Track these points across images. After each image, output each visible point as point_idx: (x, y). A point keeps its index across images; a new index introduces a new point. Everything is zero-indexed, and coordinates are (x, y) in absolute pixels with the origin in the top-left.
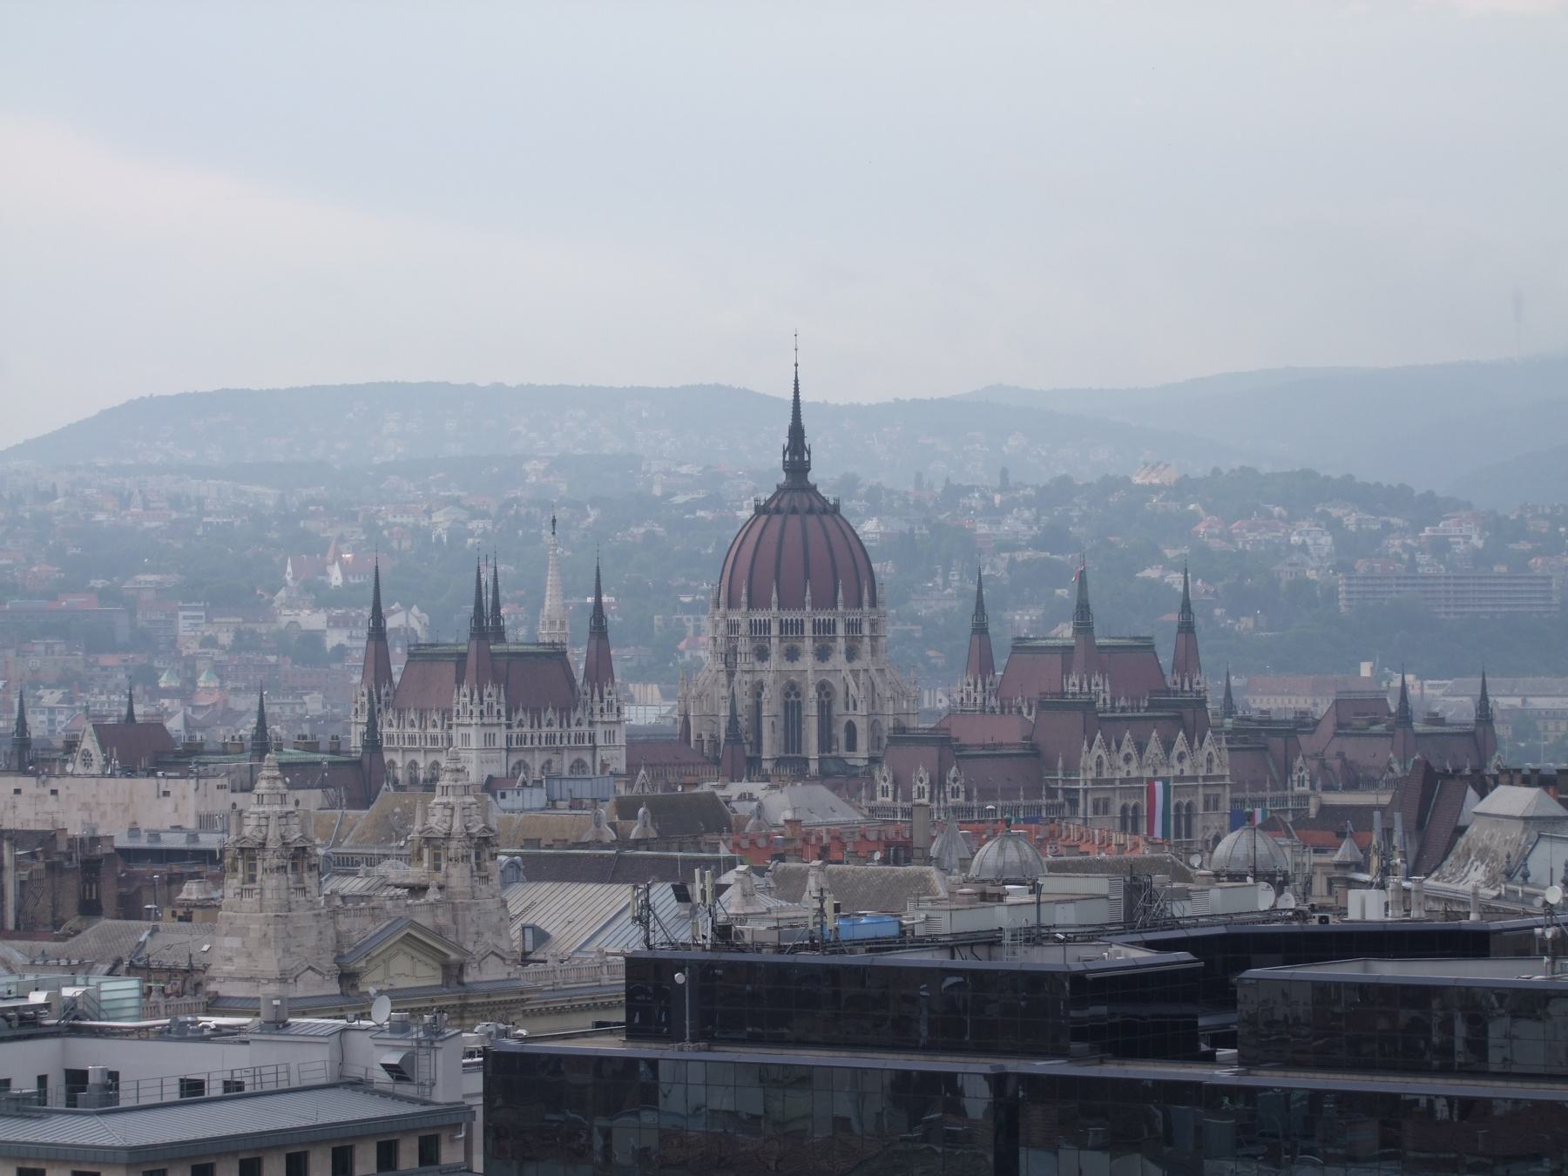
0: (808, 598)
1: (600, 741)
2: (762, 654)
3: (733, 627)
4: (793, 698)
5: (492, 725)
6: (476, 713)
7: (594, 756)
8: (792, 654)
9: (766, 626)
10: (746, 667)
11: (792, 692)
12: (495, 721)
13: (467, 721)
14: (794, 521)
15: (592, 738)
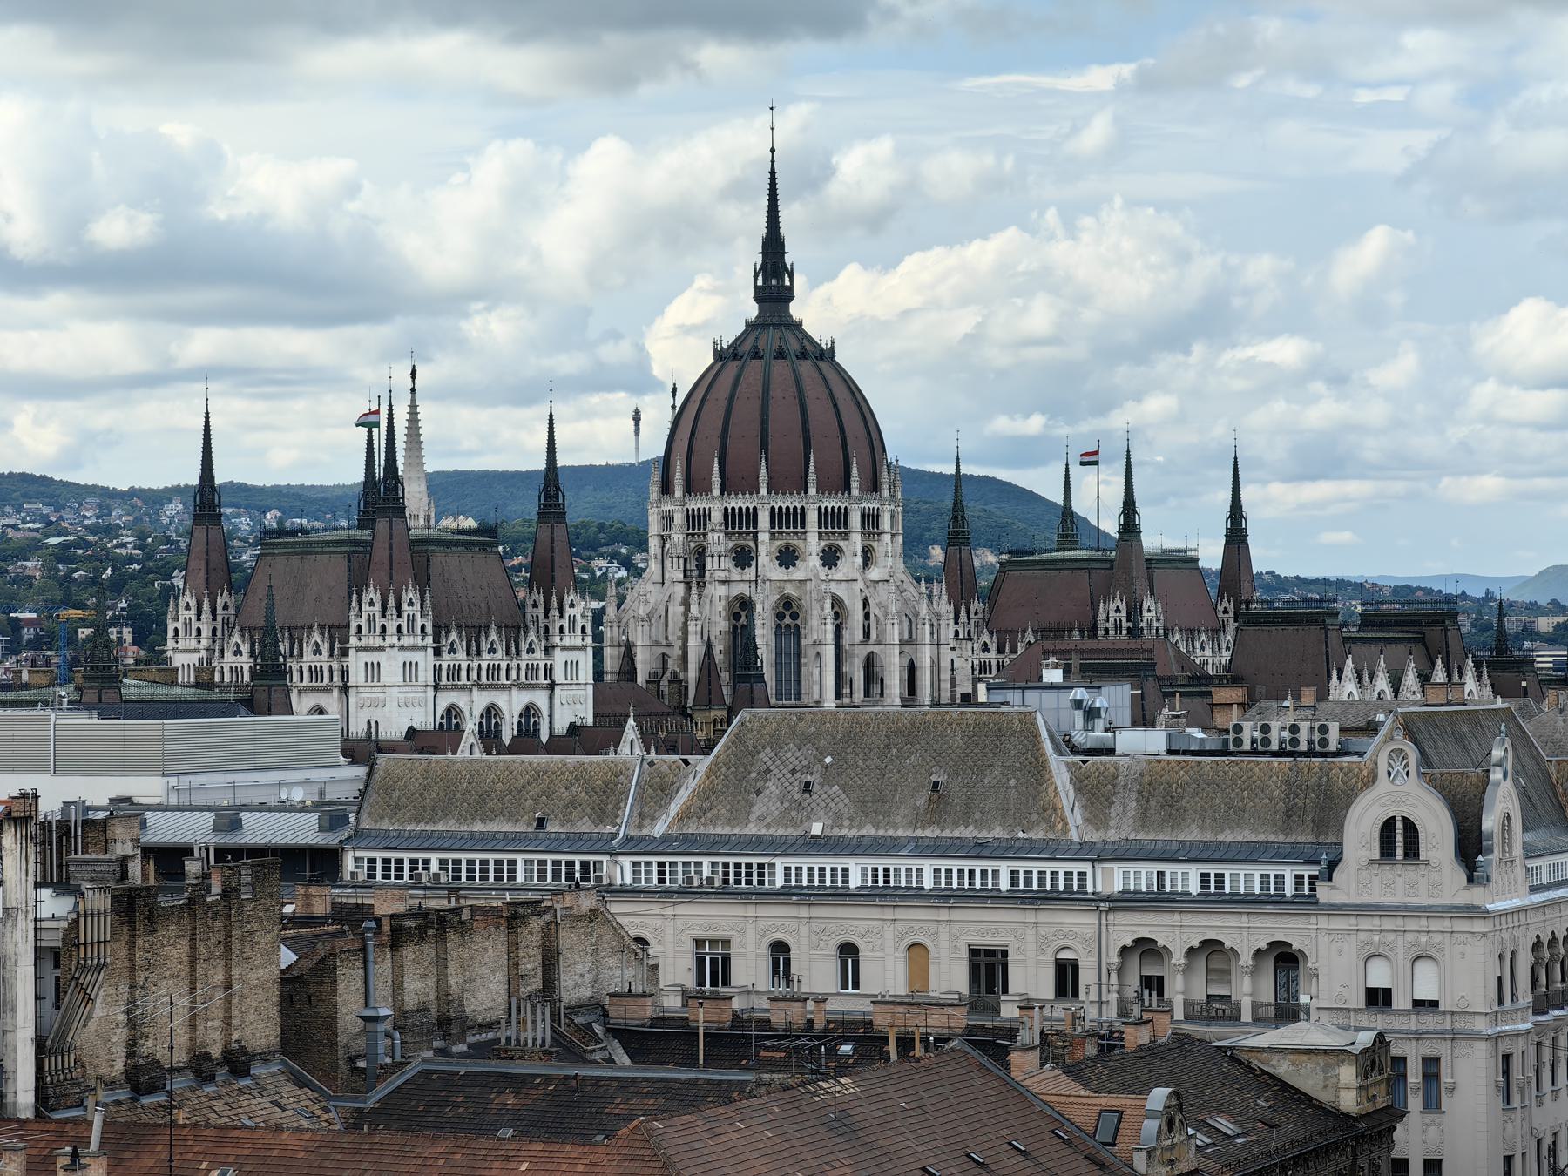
0: (812, 478)
1: (559, 676)
2: (743, 558)
3: (697, 520)
4: (788, 620)
5: (414, 648)
6: (391, 628)
7: (551, 698)
8: (788, 557)
9: (752, 516)
10: (721, 575)
11: (788, 609)
12: (418, 641)
13: (378, 641)
14: (780, 369)
15: (549, 671)
